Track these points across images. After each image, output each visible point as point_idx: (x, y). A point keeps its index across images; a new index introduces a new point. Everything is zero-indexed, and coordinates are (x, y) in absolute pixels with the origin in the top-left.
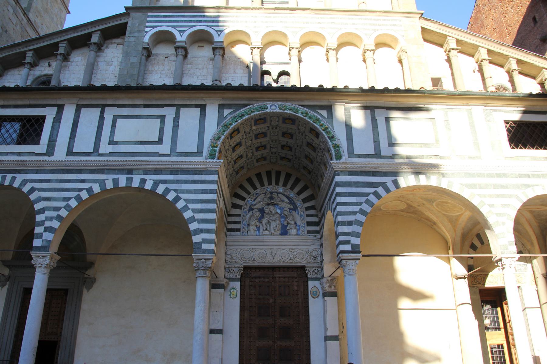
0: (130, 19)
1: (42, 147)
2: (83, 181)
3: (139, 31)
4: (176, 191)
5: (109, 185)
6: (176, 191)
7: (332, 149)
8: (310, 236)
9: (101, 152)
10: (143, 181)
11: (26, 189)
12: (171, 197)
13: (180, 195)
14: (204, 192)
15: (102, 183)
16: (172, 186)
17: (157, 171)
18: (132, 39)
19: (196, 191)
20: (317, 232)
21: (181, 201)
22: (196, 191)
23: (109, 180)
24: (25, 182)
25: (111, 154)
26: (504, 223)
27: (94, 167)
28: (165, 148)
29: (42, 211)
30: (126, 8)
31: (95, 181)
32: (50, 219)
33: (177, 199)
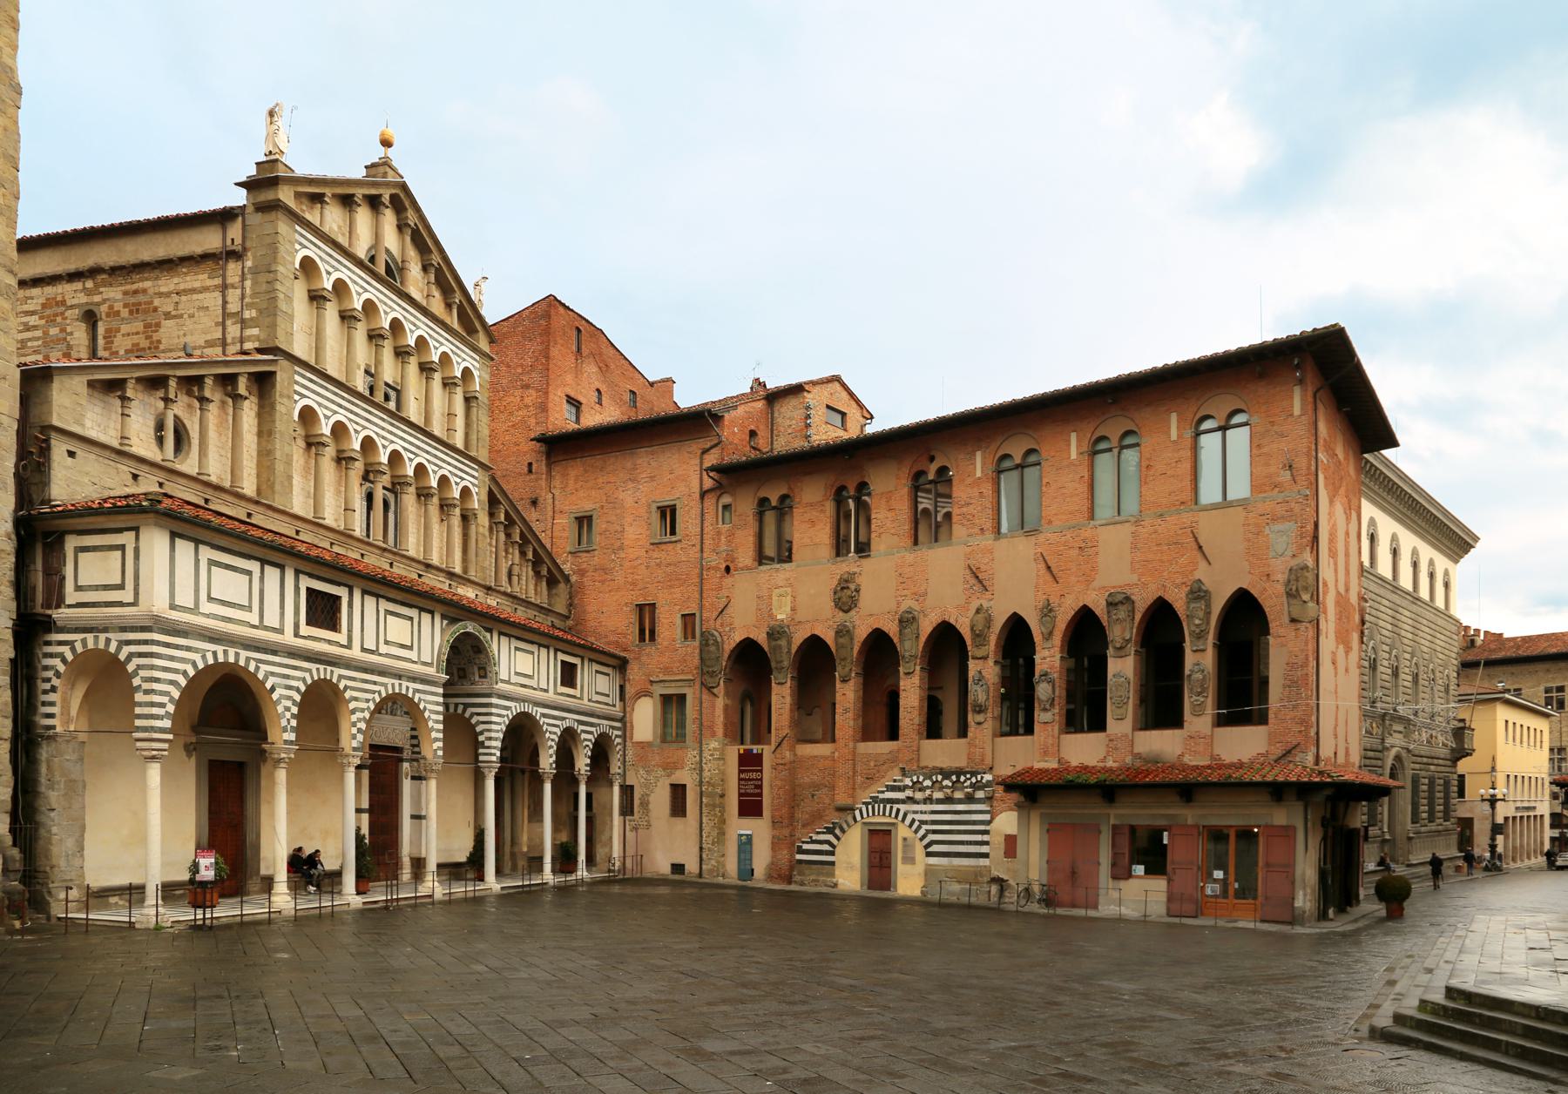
1: (341, 638)
2: (375, 683)
28: (413, 655)
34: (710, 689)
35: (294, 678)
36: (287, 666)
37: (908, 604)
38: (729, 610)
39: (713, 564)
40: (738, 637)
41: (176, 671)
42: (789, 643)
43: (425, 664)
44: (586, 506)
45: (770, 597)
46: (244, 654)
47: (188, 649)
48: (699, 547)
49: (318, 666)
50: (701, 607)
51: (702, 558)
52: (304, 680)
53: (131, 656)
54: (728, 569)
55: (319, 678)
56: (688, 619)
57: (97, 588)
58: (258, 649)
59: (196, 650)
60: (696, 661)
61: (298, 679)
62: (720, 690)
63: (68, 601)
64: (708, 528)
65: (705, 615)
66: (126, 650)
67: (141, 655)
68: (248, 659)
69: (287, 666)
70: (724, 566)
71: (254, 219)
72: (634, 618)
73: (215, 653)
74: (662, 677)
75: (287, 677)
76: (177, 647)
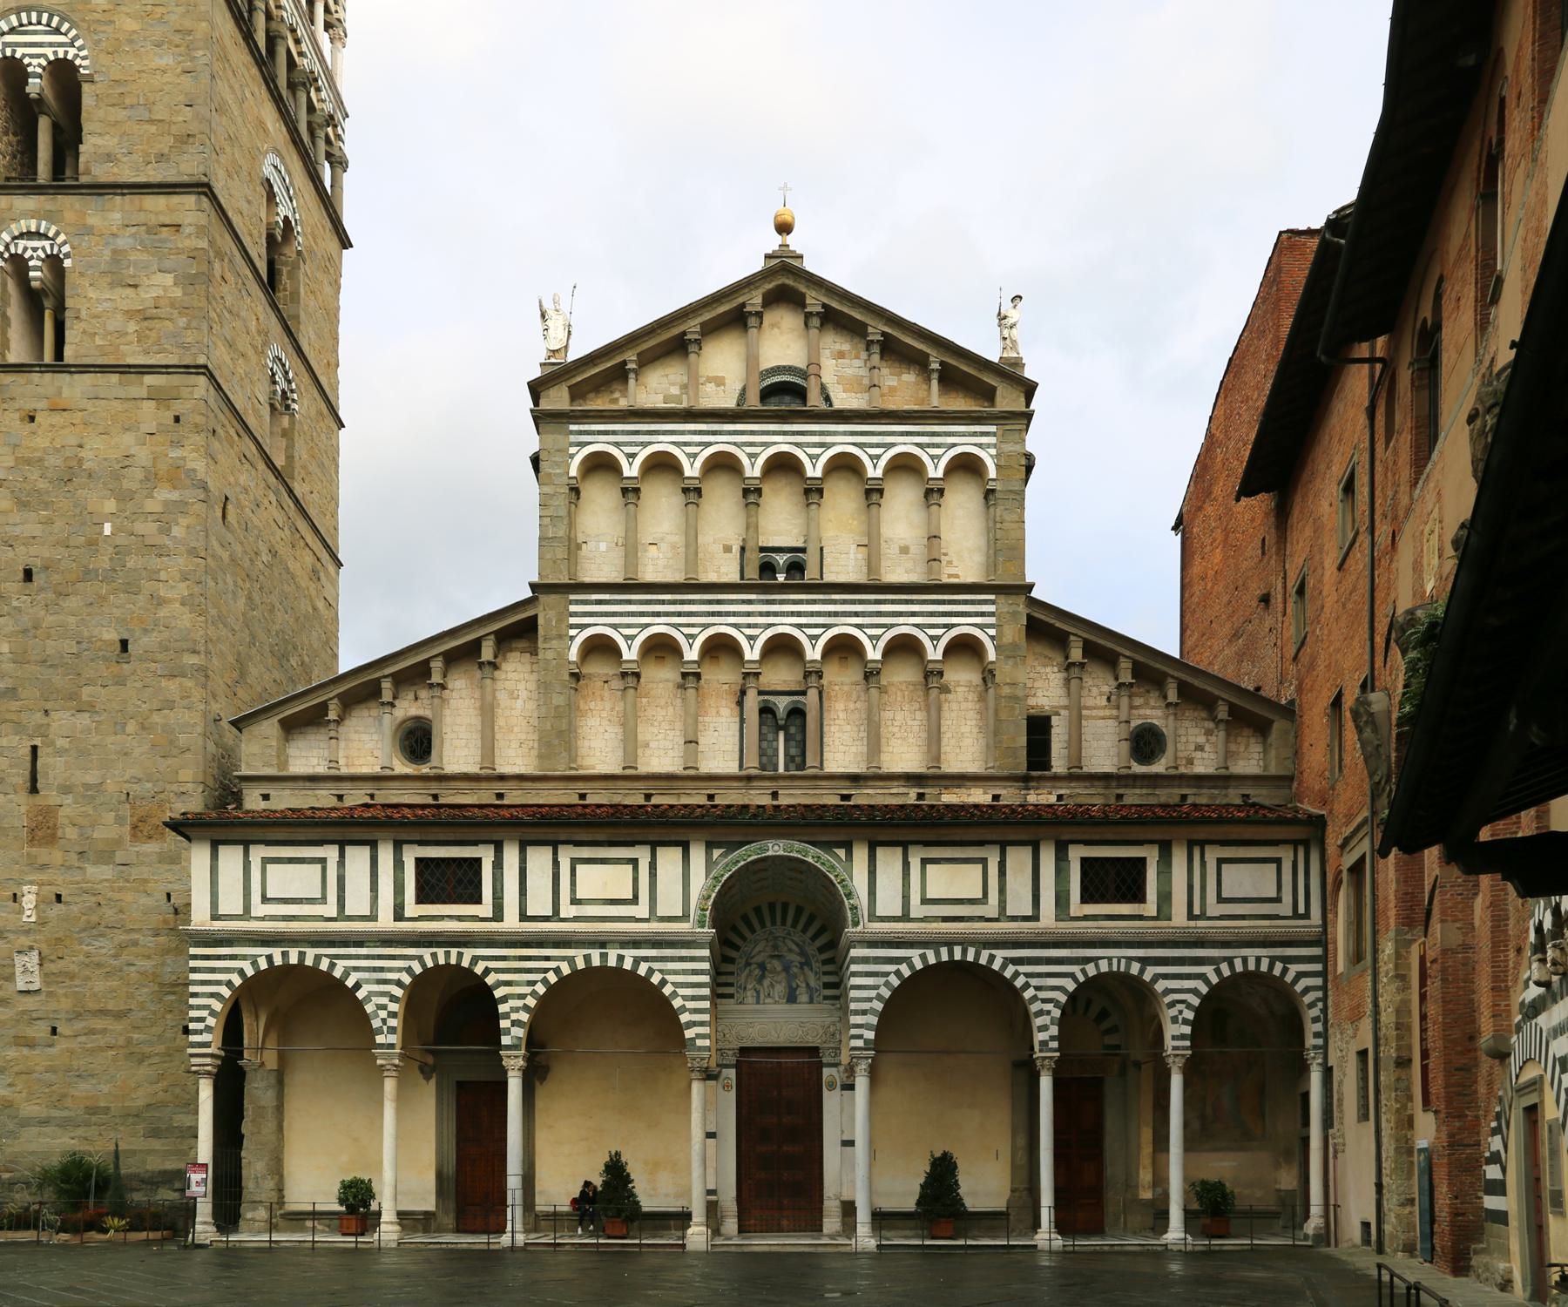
0: (541, 608)
3: (560, 637)
4: (661, 971)
5: (581, 965)
6: (661, 971)
7: (849, 911)
8: (827, 1005)
9: (562, 915)
10: (621, 958)
11: (479, 969)
12: (655, 979)
13: (666, 977)
14: (695, 972)
15: (571, 961)
16: (656, 965)
17: (636, 943)
18: (550, 655)
19: (685, 972)
20: (837, 998)
21: (669, 985)
22: (685, 972)
23: (578, 954)
24: (475, 960)
25: (576, 919)
26: (1049, 1012)
27: (558, 939)
29: (505, 999)
30: (533, 586)
31: (563, 959)
32: (516, 1010)
33: (663, 982)
35: (390, 970)
36: (380, 957)
41: (218, 983)
46: (311, 954)
47: (233, 957)
49: (434, 950)
52: (409, 970)
55: (458, 965)
58: (332, 944)
59: (244, 958)
61: (400, 970)
68: (318, 958)
69: (380, 957)
73: (269, 958)
75: (382, 969)
76: (219, 958)
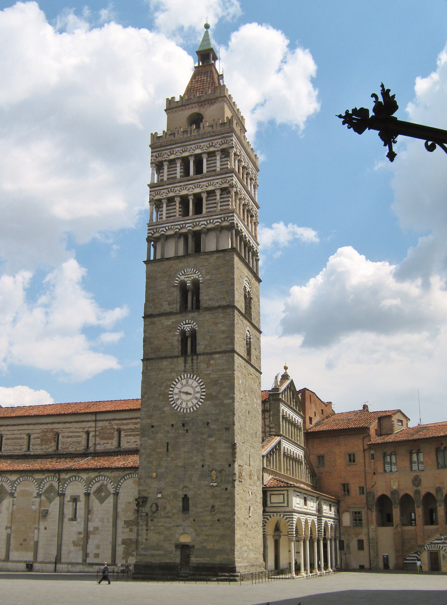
34: (370, 510)
37: (438, 485)
38: (376, 485)
39: (369, 471)
40: (380, 494)
42: (398, 496)
43: (315, 511)
44: (322, 453)
45: (390, 482)
48: (364, 466)
50: (366, 484)
51: (365, 470)
53: (287, 518)
54: (374, 473)
56: (362, 489)
57: (276, 503)
60: (365, 501)
62: (374, 510)
63: (268, 506)
64: (367, 460)
65: (368, 487)
66: (285, 517)
67: (290, 518)
70: (373, 472)
71: (272, 402)
72: (342, 488)
74: (353, 506)
